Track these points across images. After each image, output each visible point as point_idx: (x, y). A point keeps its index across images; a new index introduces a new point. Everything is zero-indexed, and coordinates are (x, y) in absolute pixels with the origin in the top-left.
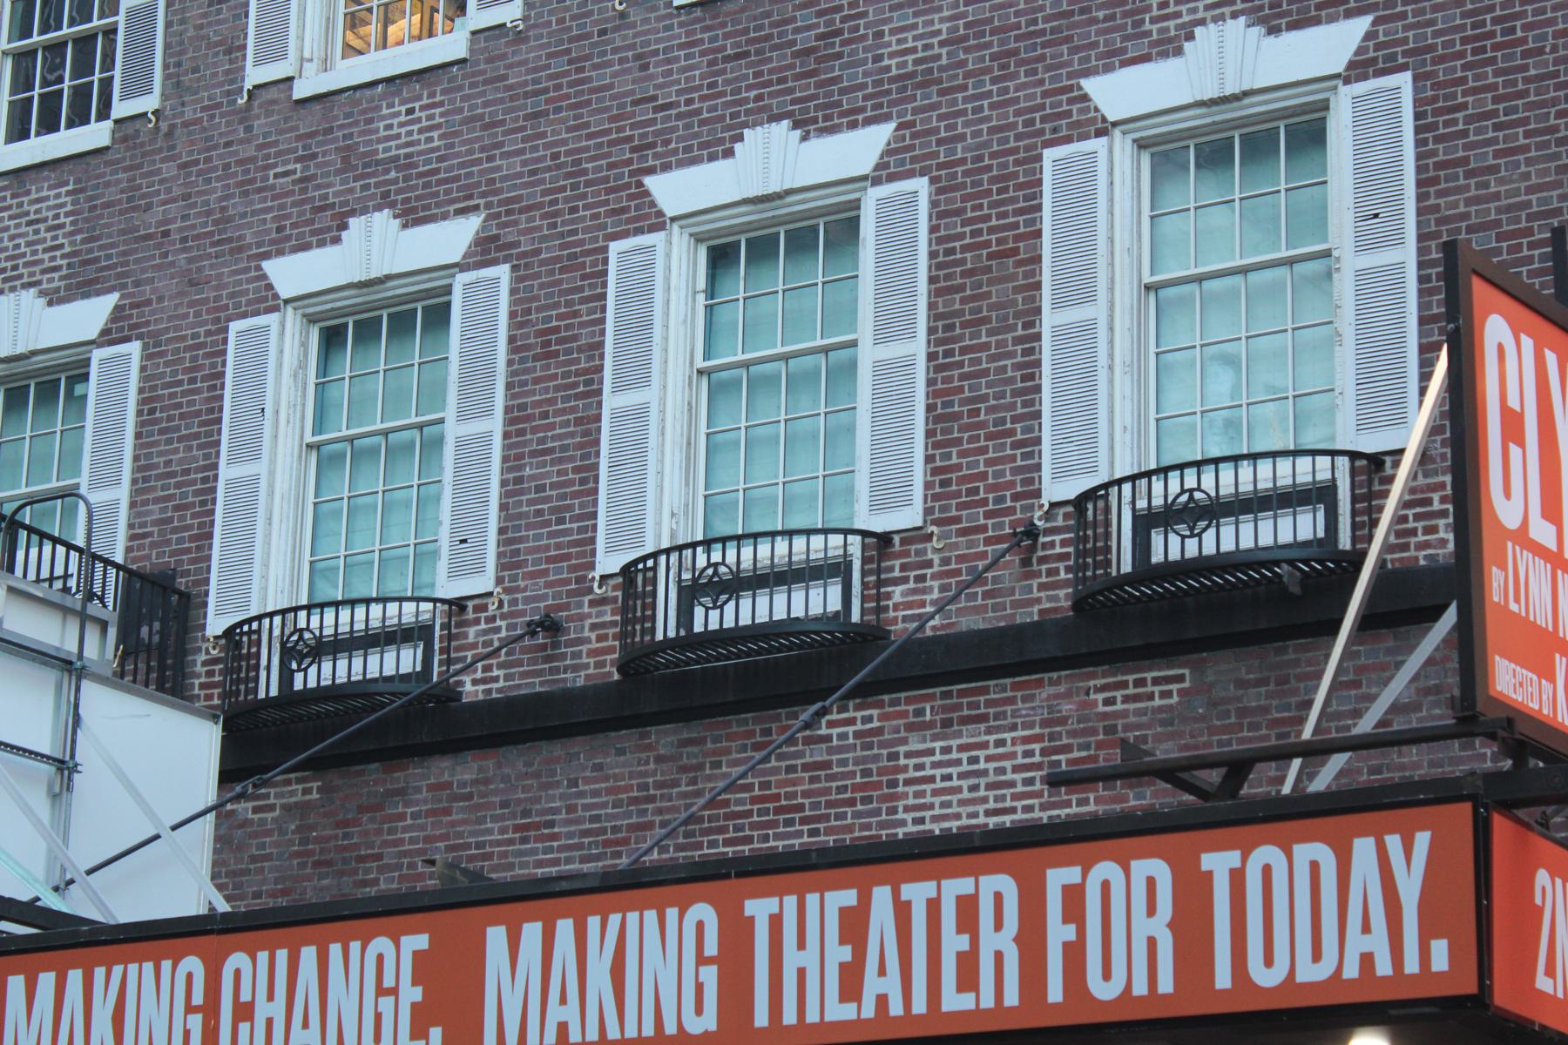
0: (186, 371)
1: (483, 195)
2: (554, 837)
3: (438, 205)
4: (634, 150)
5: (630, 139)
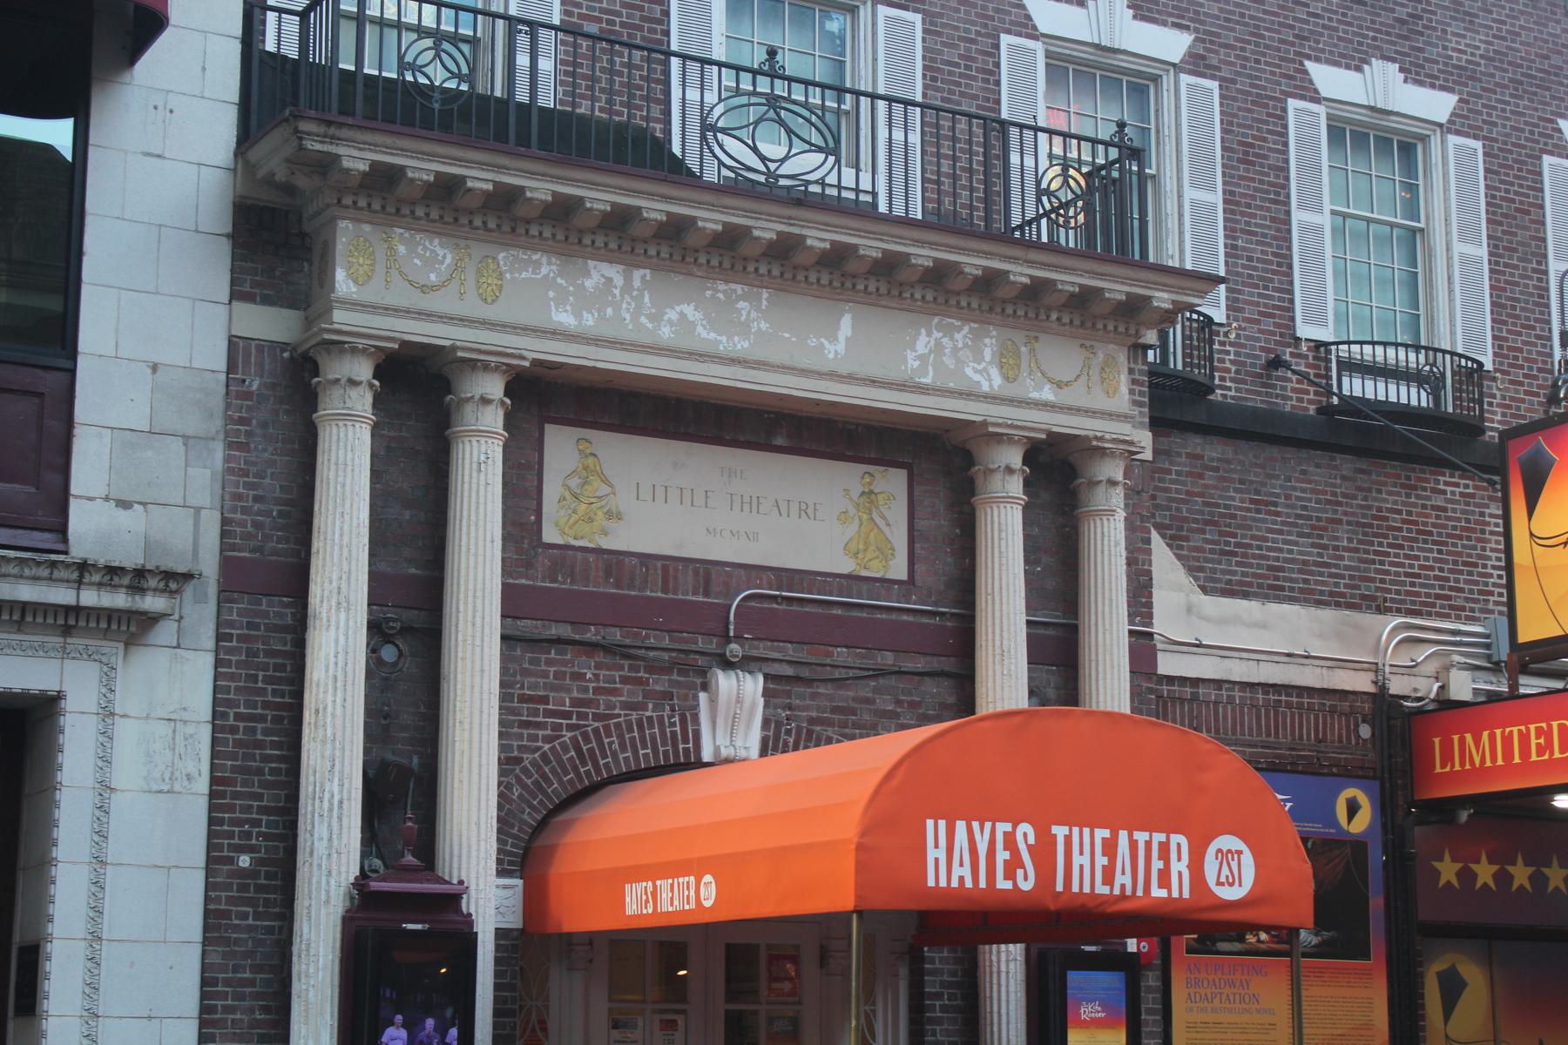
0: (960, 57)
1: (1191, 20)
2: (1277, 514)
3: (1158, 12)
4: (1295, 36)
5: (1292, 27)
